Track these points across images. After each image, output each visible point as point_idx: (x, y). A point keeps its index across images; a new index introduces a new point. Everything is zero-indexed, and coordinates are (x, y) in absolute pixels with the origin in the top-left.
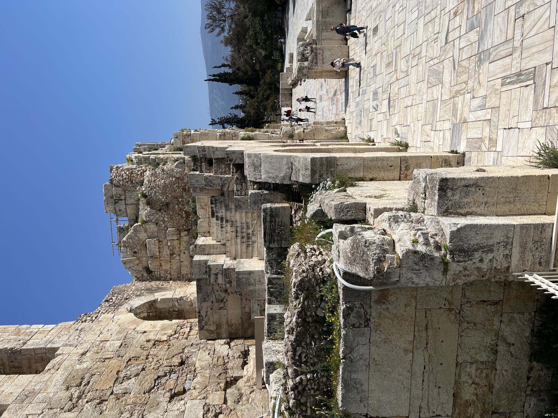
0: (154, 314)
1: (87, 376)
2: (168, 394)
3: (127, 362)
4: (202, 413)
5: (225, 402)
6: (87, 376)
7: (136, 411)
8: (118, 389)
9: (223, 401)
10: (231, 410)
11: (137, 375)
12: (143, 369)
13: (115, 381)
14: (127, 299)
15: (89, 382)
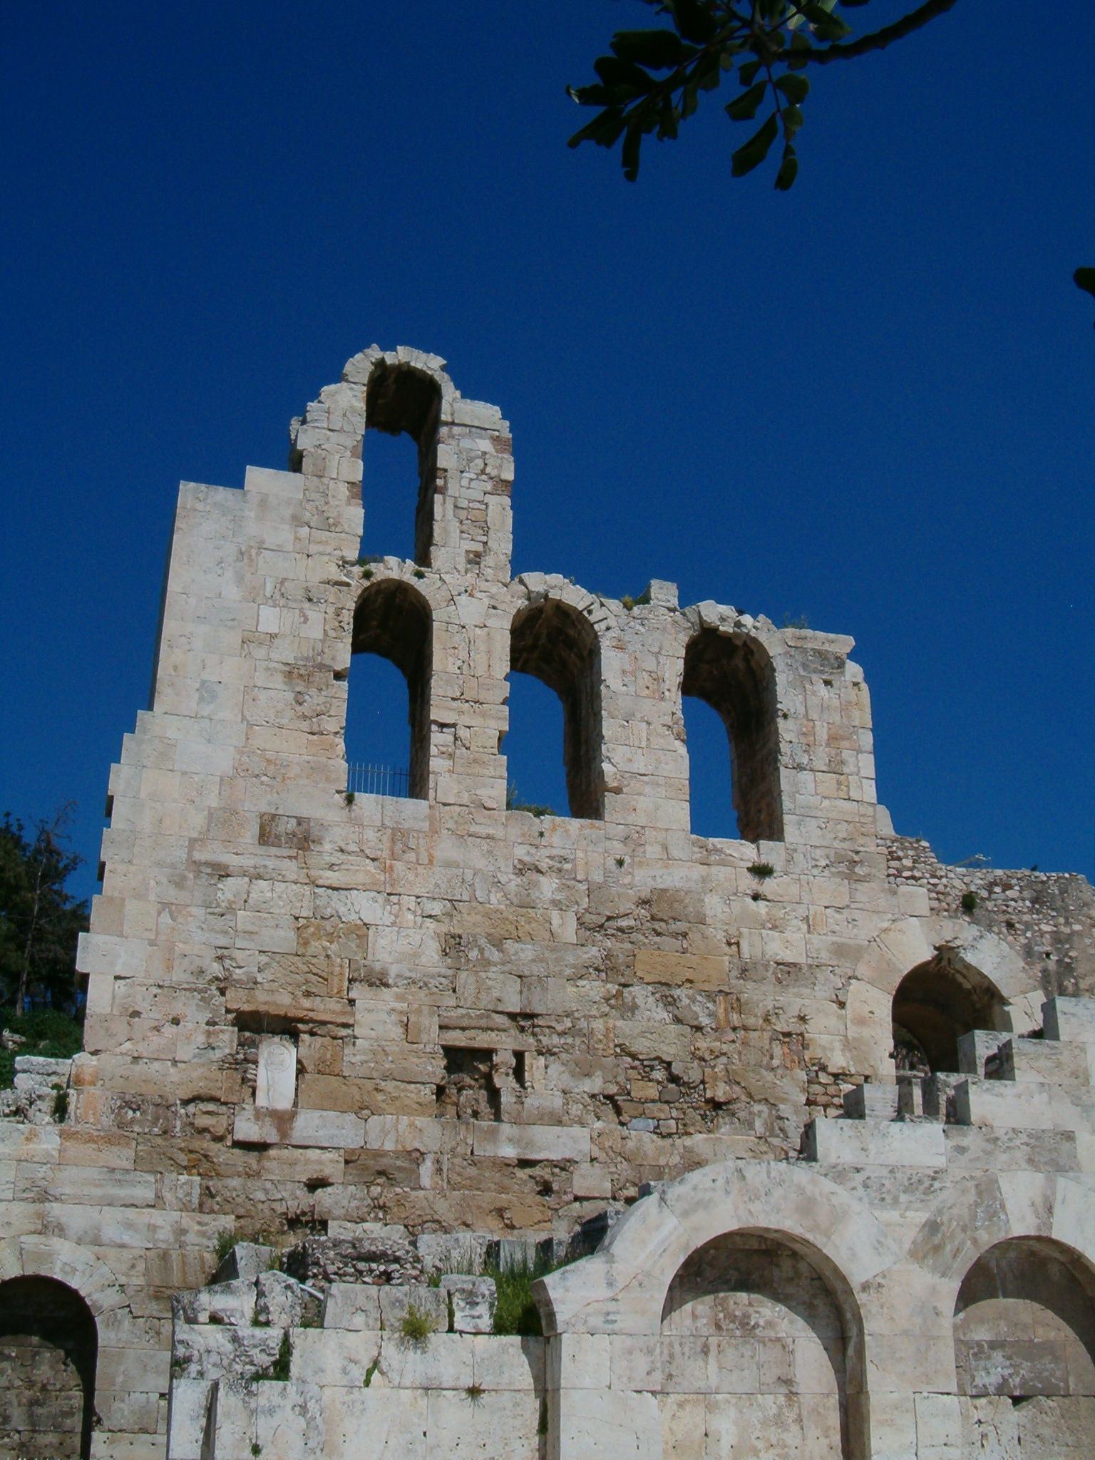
0: (978, 1006)
1: (674, 927)
2: (613, 1089)
3: (721, 991)
4: (553, 1156)
5: (577, 1199)
6: (681, 926)
7: (570, 1040)
8: (639, 993)
9: (580, 1194)
10: (556, 1210)
11: (678, 1020)
12: (699, 1028)
13: (660, 983)
14: (1010, 925)
15: (658, 934)
